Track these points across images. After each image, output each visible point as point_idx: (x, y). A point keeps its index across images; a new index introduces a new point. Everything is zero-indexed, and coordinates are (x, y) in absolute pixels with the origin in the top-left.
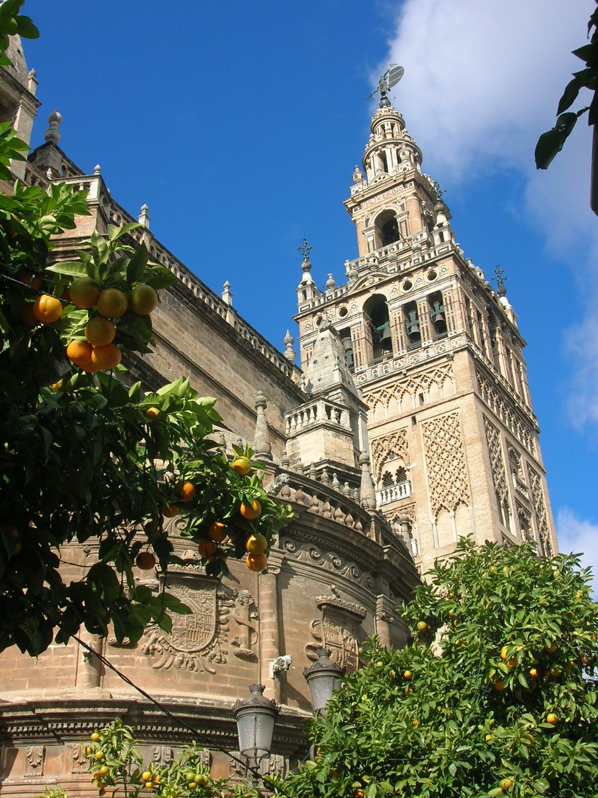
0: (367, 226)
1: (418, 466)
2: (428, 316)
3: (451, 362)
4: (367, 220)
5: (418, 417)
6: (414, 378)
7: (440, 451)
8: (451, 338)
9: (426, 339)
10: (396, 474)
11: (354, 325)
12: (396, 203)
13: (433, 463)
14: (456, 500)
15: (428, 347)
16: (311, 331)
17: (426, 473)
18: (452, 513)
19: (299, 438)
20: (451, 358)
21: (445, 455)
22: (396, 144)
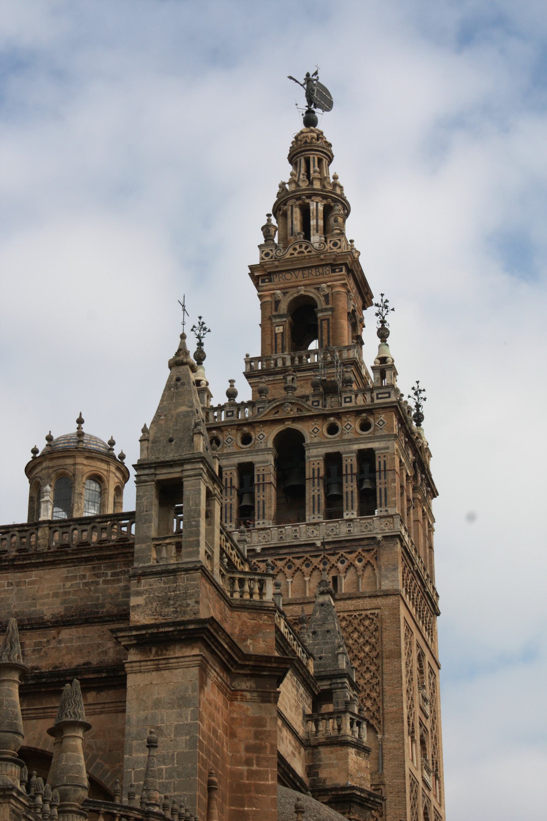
0: (276, 310)
6: (328, 554)
9: (350, 507)
12: (318, 289)
15: (351, 520)
19: (321, 749)
22: (325, 197)
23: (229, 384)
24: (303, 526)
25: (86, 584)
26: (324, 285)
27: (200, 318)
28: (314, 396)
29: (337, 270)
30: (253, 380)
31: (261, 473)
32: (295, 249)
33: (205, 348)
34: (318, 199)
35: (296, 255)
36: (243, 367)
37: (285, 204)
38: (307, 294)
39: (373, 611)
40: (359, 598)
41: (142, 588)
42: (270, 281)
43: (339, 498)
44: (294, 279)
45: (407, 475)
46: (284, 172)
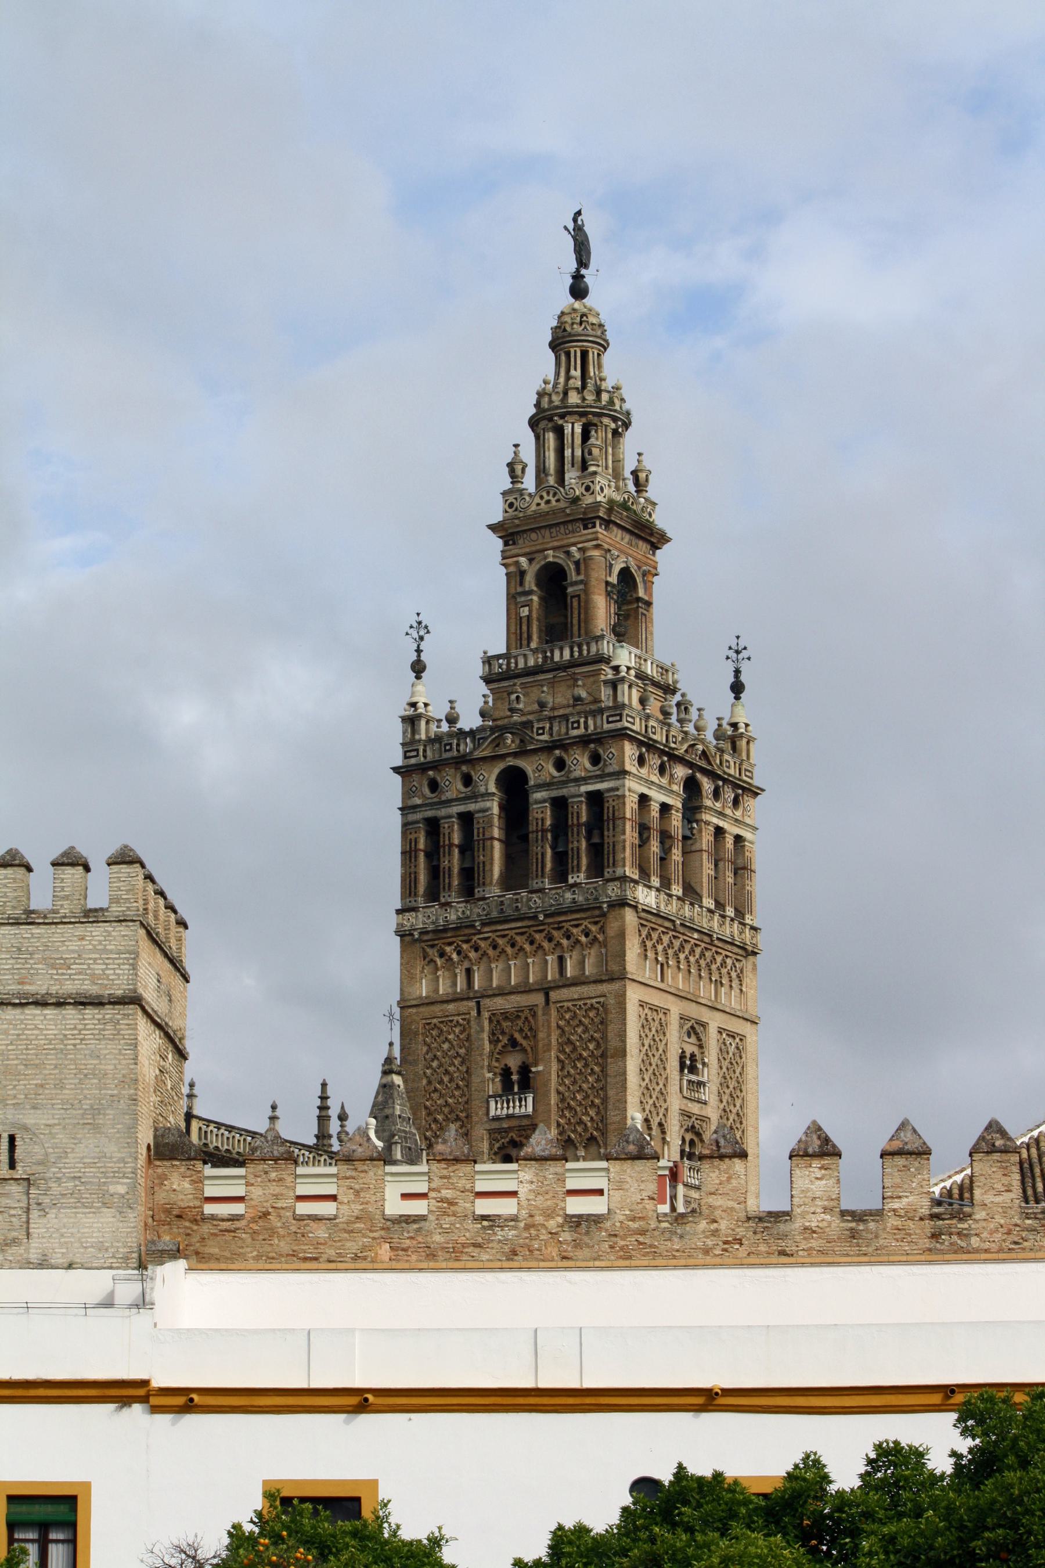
0: (522, 584)
3: (603, 920)
4: (522, 573)
5: (554, 995)
6: (554, 929)
8: (608, 880)
11: (479, 811)
15: (576, 885)
20: (604, 915)
22: (582, 414)
23: (449, 705)
26: (573, 549)
27: (418, 614)
28: (539, 721)
29: (590, 526)
31: (481, 825)
32: (542, 497)
33: (423, 657)
34: (577, 417)
36: (479, 669)
37: (537, 425)
38: (556, 560)
39: (598, 1000)
40: (584, 983)
42: (514, 544)
43: (566, 853)
44: (540, 541)
45: (665, 808)
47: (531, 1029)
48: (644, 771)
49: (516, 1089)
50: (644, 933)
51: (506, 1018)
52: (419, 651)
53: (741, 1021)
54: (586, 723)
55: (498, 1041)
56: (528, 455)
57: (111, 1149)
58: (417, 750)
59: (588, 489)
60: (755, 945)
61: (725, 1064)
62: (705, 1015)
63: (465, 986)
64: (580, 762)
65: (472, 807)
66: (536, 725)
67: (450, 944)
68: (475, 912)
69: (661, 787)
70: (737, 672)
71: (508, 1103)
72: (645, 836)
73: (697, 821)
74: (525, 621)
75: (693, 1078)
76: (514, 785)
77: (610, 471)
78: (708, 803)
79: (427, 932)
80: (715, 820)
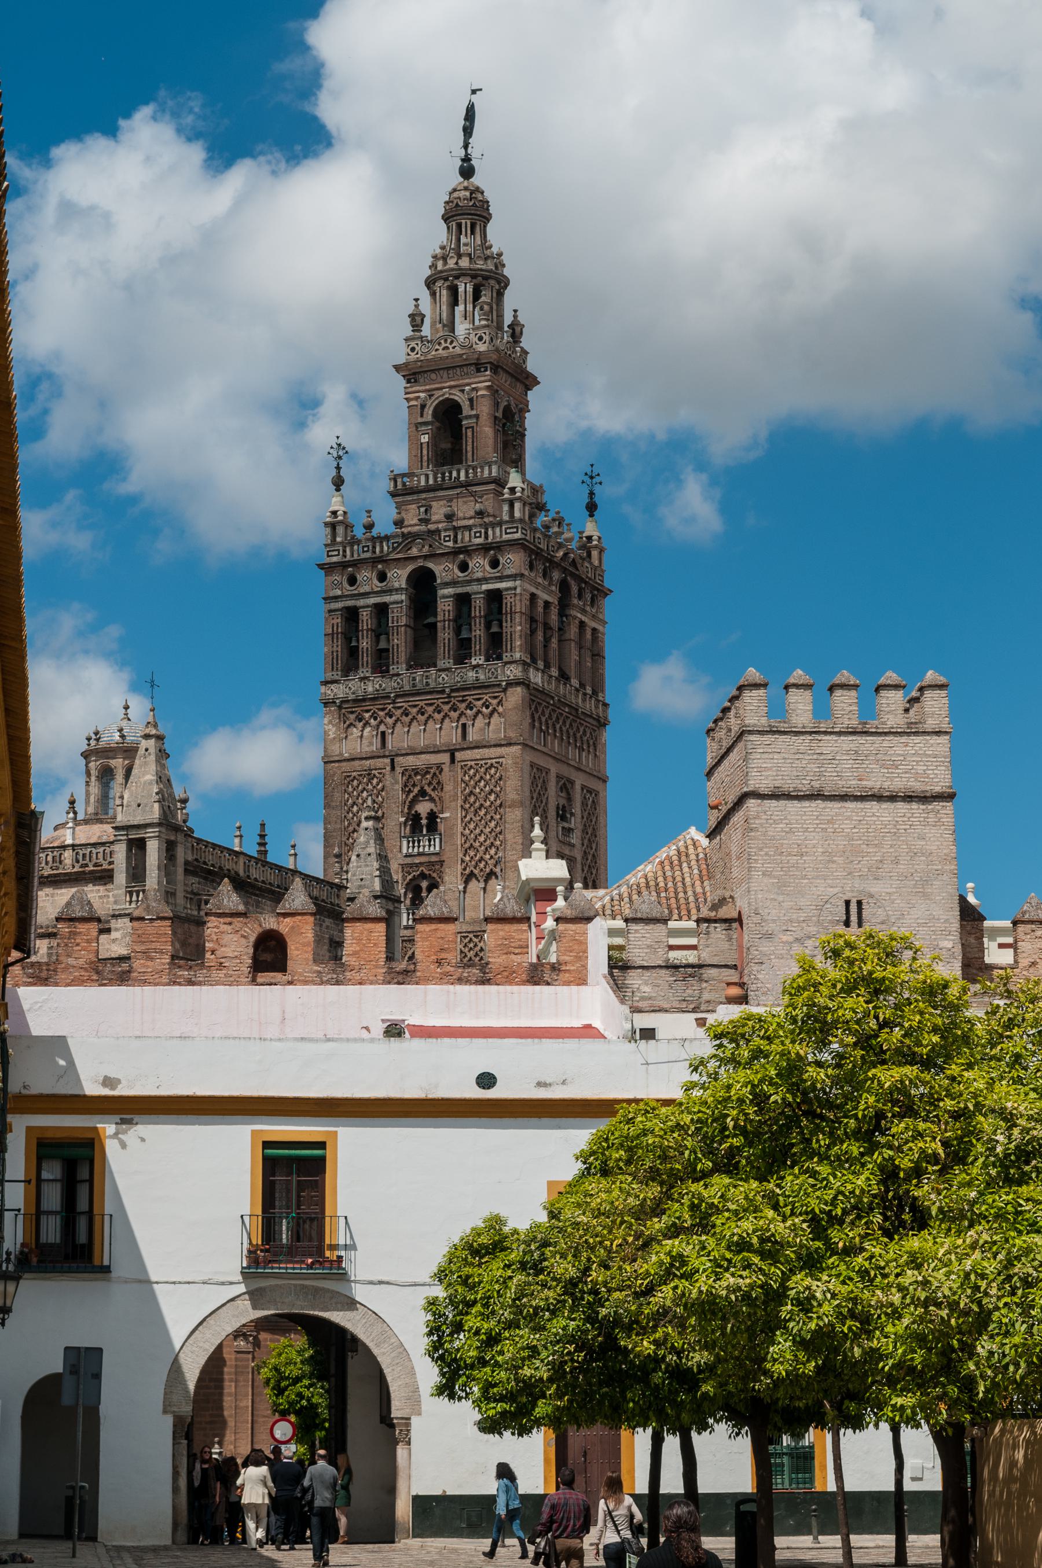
0: (422, 416)
1: (451, 815)
2: (482, 620)
4: (423, 407)
7: (477, 804)
10: (427, 818)
12: (463, 391)
13: (468, 818)
14: (488, 870)
15: (478, 666)
16: (339, 593)
17: (460, 829)
18: (482, 885)
20: (505, 690)
21: (482, 812)
22: (474, 277)
24: (433, 671)
25: (100, 897)
26: (467, 388)
30: (399, 499)
35: (440, 351)
37: (434, 283)
38: (452, 397)
40: (485, 747)
41: (119, 926)
42: (416, 381)
45: (547, 604)
46: (439, 235)
47: (439, 783)
48: (533, 574)
49: (425, 832)
50: (533, 707)
51: (416, 774)
52: (338, 468)
53: (596, 779)
54: (486, 533)
55: (410, 791)
56: (426, 306)
57: (937, 912)
58: (338, 550)
59: (480, 339)
60: (606, 718)
61: (586, 814)
62: (574, 775)
63: (379, 746)
64: (479, 565)
65: (387, 599)
66: (443, 534)
67: (367, 711)
68: (389, 685)
69: (544, 588)
70: (592, 494)
71: (414, 843)
72: (534, 626)
73: (566, 616)
74: (425, 446)
75: (566, 825)
76: (423, 584)
77: (495, 324)
78: (575, 601)
79: (348, 701)
80: (579, 615)
